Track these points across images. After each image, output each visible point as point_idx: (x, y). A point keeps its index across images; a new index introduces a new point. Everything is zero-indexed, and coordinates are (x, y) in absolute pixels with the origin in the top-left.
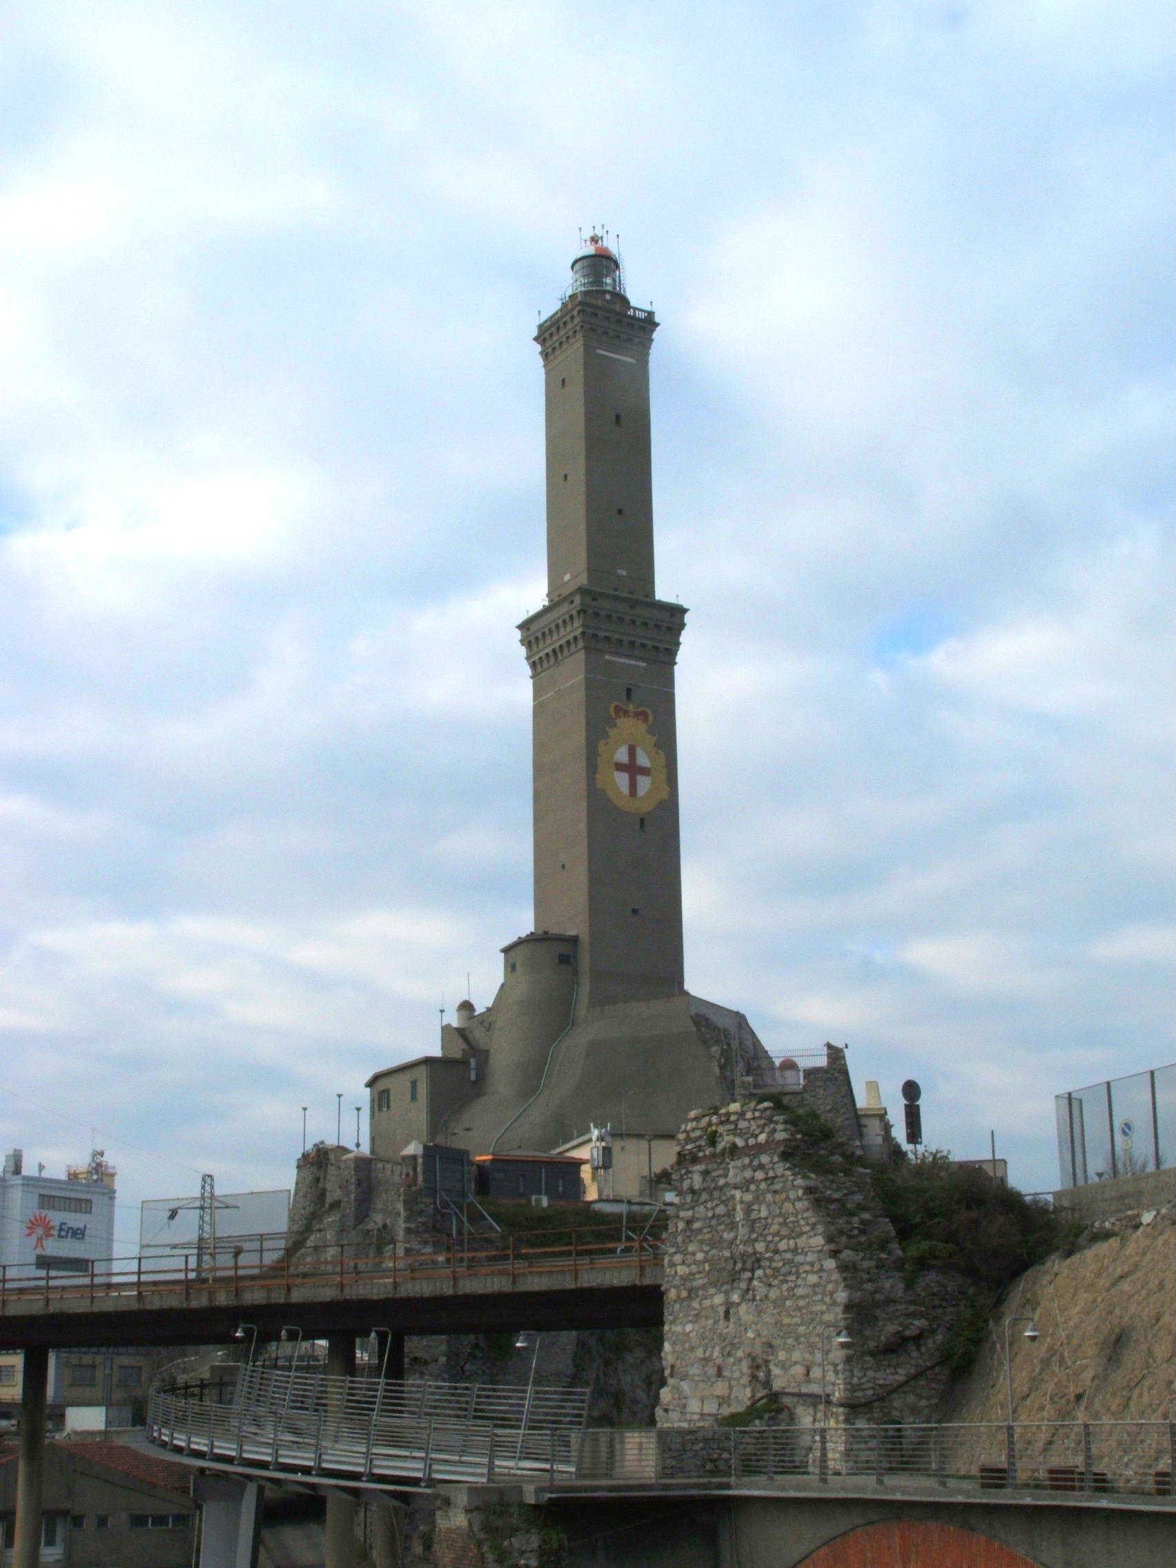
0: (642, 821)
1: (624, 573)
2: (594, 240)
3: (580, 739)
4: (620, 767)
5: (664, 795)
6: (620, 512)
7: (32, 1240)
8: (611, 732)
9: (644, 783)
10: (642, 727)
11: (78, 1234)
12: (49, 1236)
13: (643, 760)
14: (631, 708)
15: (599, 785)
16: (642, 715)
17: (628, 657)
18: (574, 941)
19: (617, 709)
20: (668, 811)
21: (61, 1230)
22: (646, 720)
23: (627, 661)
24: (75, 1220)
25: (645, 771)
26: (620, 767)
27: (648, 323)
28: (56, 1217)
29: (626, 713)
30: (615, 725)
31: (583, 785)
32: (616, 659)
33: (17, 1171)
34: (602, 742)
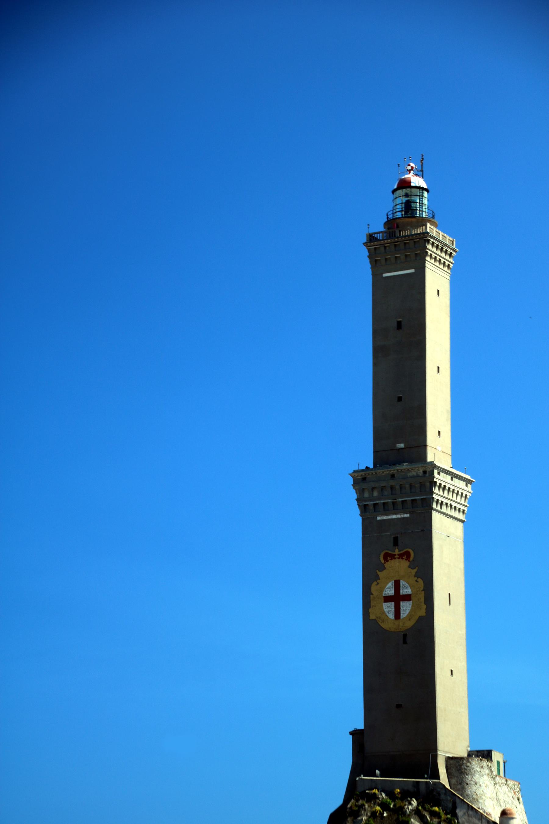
0: (405, 636)
1: (402, 445)
4: (387, 599)
6: (400, 399)
8: (381, 574)
9: (406, 607)
10: (407, 563)
13: (406, 590)
14: (397, 552)
15: (372, 617)
16: (406, 555)
17: (396, 514)
23: (394, 517)
25: (407, 598)
26: (387, 599)
29: (393, 557)
30: (385, 568)
32: (385, 518)
34: (375, 583)
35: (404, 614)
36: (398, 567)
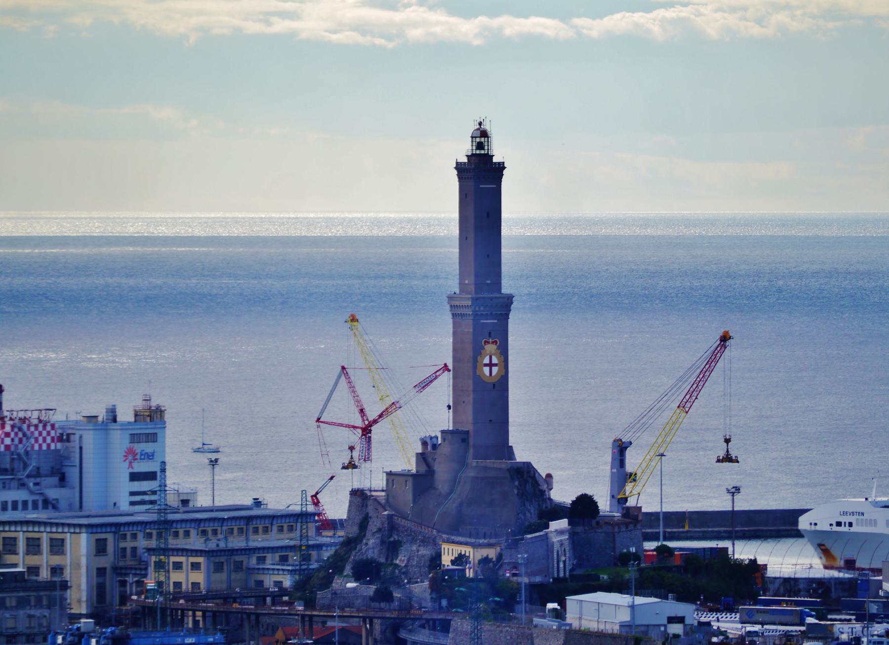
1: (489, 282)
2: (480, 124)
3: (471, 354)
4: (486, 365)
5: (503, 373)
7: (127, 463)
9: (495, 370)
11: (150, 456)
12: (135, 459)
18: (467, 432)
19: (485, 342)
20: (503, 381)
21: (142, 455)
22: (496, 342)
24: (148, 447)
27: (501, 167)
28: (140, 447)
29: (489, 343)
31: (471, 373)
33: (115, 420)
35: (494, 373)
36: (491, 348)
